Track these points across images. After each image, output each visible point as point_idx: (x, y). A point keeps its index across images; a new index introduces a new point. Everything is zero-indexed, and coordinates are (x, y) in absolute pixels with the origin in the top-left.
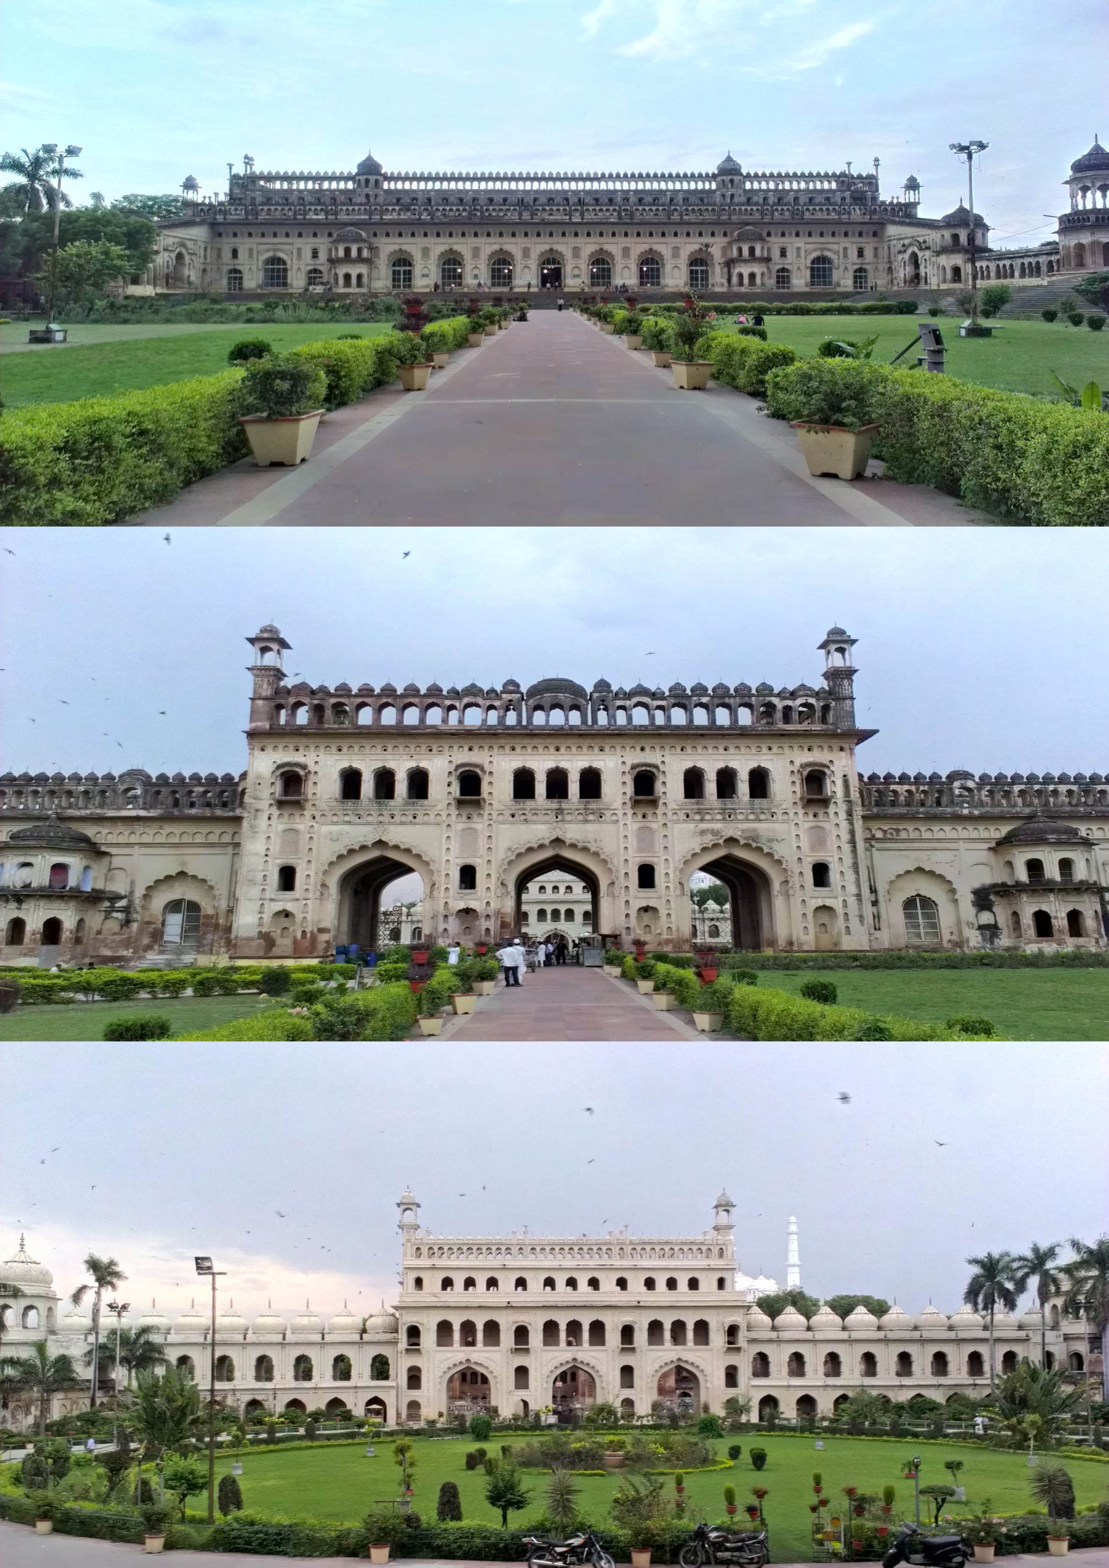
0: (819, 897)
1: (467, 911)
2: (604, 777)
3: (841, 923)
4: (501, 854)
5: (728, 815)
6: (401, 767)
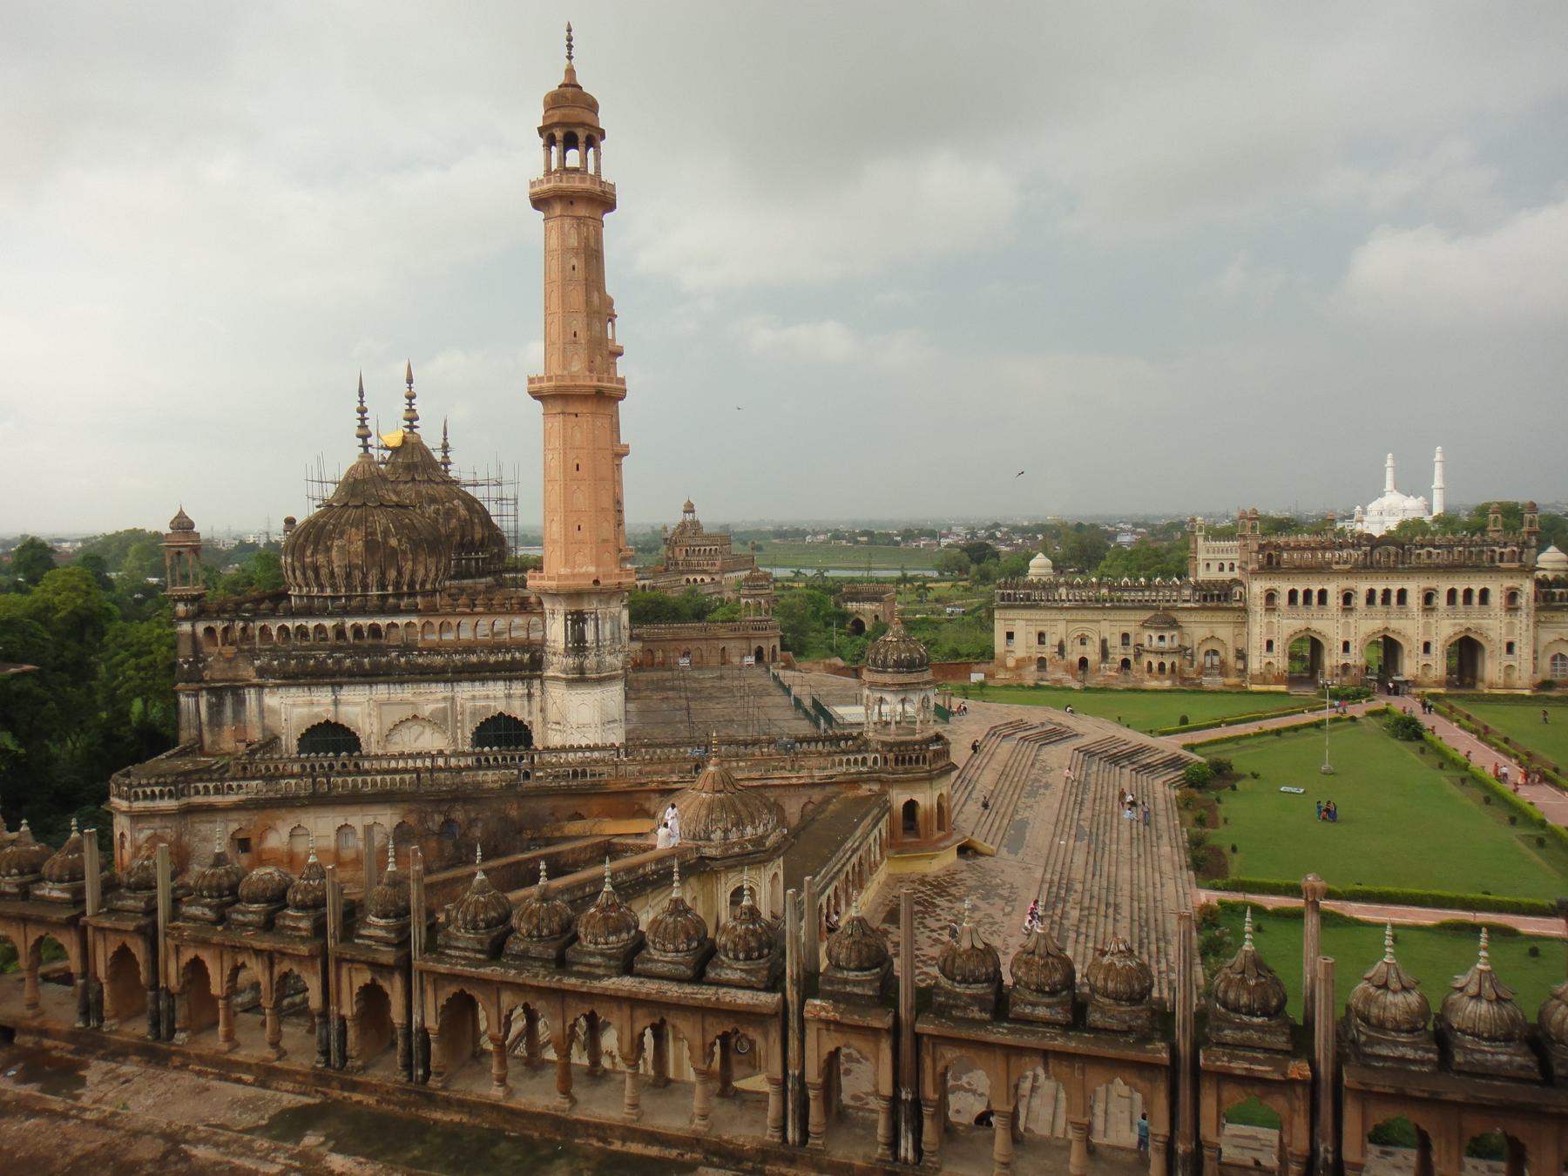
0: (1508, 660)
1: (1346, 667)
2: (1409, 594)
3: (1516, 674)
4: (1362, 635)
5: (1467, 616)
6: (1315, 589)
